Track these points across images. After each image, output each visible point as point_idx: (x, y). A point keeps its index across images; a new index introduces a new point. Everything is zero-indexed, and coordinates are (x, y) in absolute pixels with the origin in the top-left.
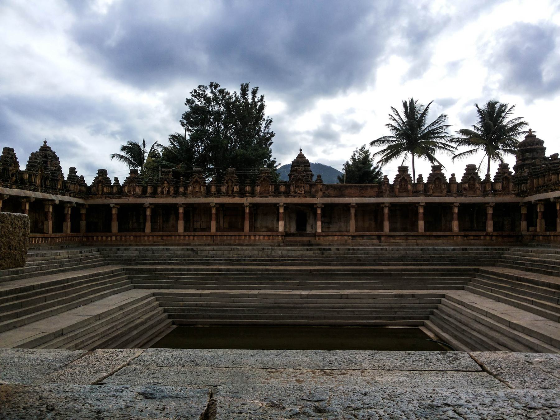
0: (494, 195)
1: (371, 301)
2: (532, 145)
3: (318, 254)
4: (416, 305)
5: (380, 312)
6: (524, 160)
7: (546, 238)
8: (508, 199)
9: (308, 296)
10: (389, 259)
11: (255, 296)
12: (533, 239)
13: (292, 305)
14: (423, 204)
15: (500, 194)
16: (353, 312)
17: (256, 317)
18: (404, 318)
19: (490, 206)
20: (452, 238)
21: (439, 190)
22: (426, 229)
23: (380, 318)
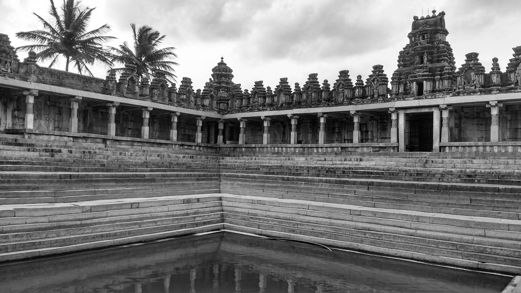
0: (204, 110)
1: (159, 209)
2: (226, 72)
3: (46, 156)
4: (208, 209)
5: (181, 219)
6: (220, 83)
7: (250, 149)
8: (213, 115)
9: (91, 209)
10: (135, 165)
11: (13, 213)
12: (234, 151)
13: (79, 223)
14: (151, 109)
15: (208, 109)
16: (155, 222)
17: (33, 245)
18: (205, 224)
19: (201, 119)
20: (171, 146)
21: (161, 98)
22: (151, 136)
23: (185, 226)
